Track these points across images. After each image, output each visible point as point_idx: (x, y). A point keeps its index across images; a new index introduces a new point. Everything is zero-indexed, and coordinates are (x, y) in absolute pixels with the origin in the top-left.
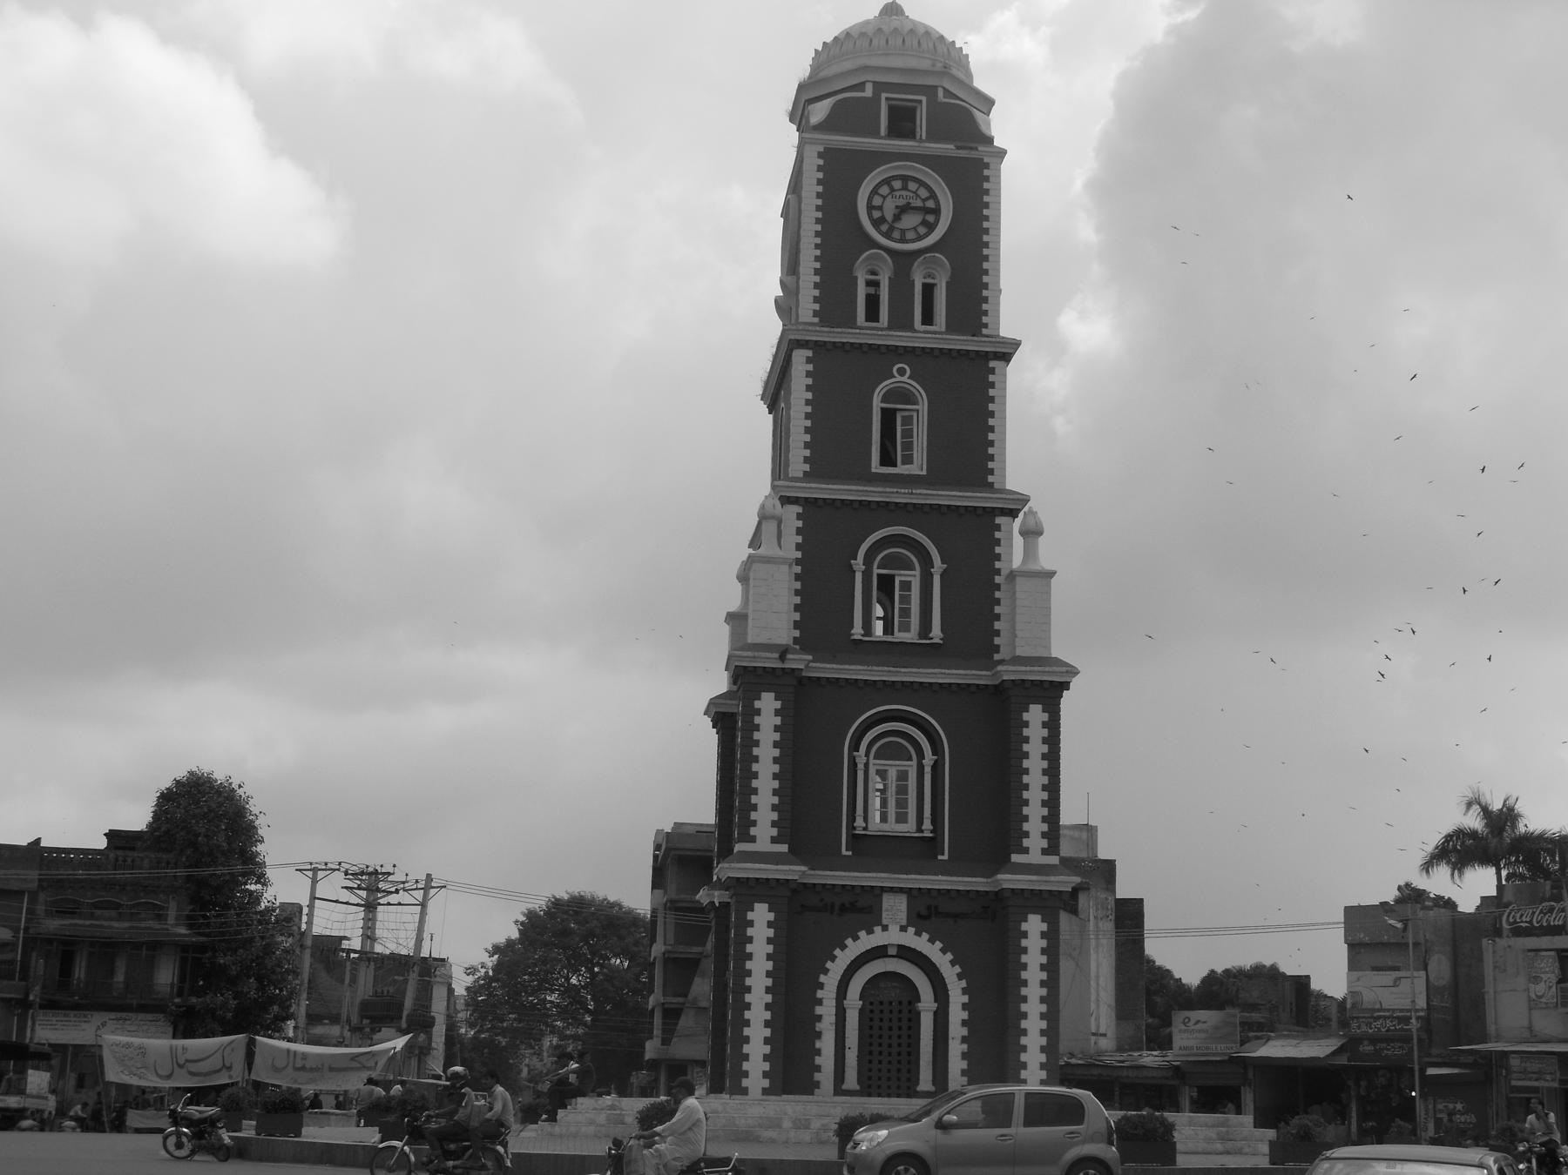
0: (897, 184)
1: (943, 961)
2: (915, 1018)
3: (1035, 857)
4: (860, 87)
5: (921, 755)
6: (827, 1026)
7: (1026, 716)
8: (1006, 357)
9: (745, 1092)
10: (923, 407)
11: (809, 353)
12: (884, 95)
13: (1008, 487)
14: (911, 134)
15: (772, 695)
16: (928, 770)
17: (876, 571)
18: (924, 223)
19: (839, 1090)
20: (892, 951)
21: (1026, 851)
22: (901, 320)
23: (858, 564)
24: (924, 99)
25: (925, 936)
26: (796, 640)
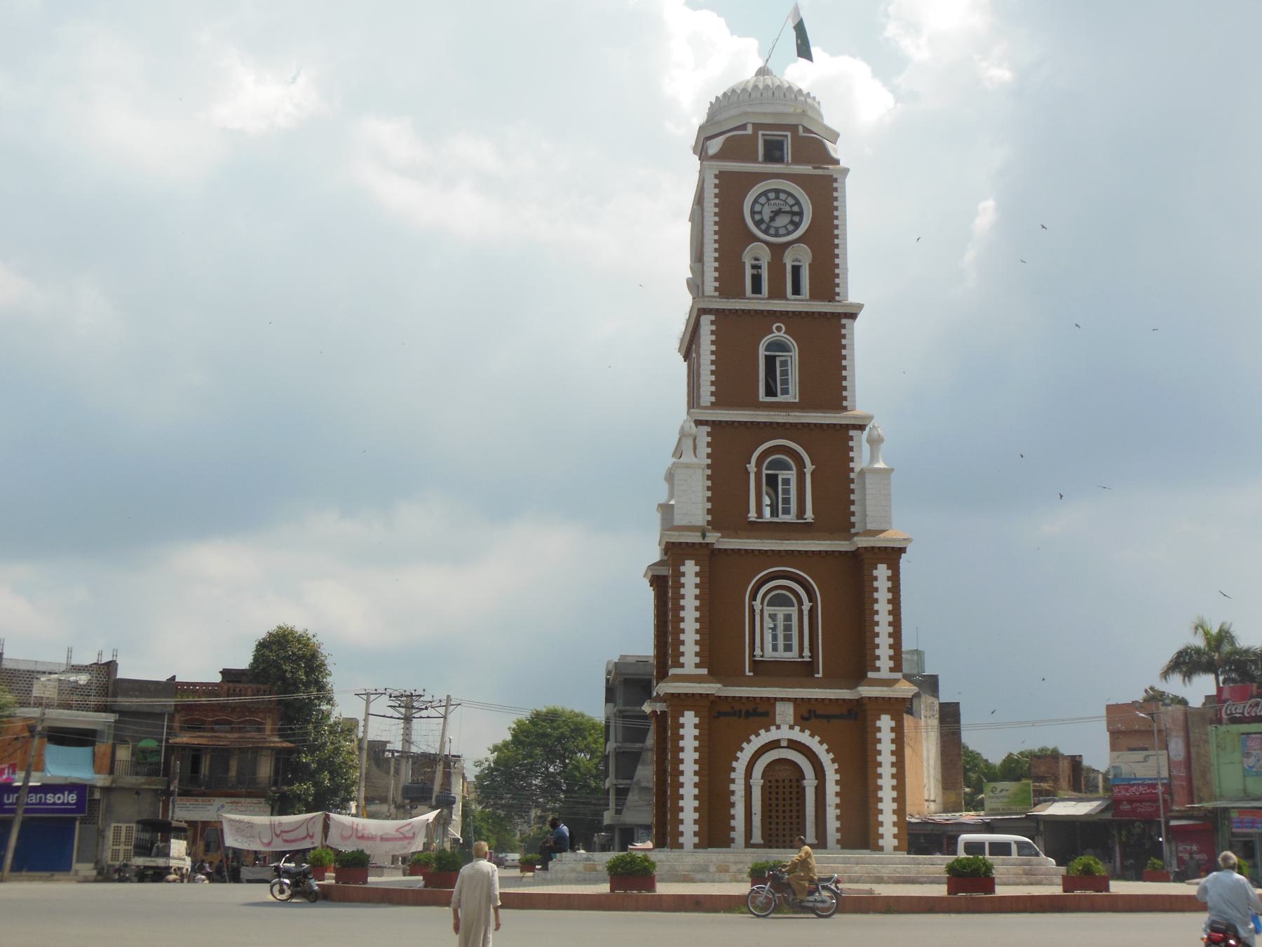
0: (772, 195)
1: (821, 750)
2: (802, 790)
3: (884, 674)
4: (743, 127)
7: (875, 573)
8: (853, 316)
9: (681, 846)
10: (795, 353)
11: (713, 317)
12: (760, 133)
14: (780, 160)
16: (806, 613)
17: (765, 472)
18: (792, 222)
19: (748, 844)
20: (784, 744)
21: (878, 669)
23: (752, 467)
24: (789, 134)
25: (807, 732)
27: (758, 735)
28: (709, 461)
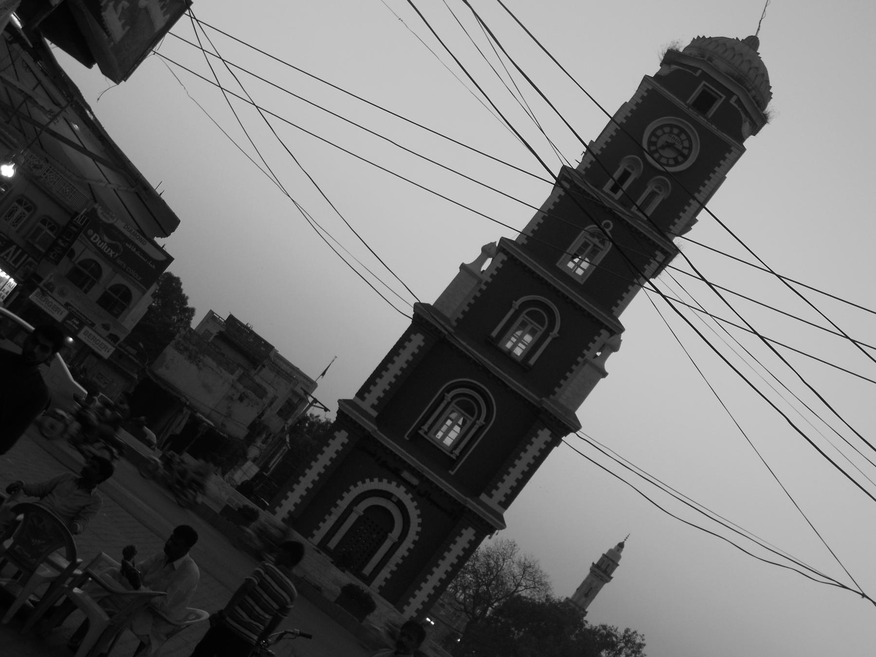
0: (676, 131)
2: (385, 537)
3: (493, 503)
4: (696, 69)
5: (478, 418)
6: (337, 513)
7: (540, 432)
9: (274, 513)
12: (704, 82)
13: (619, 319)
16: (477, 427)
18: (675, 159)
21: (491, 496)
22: (628, 201)
23: (517, 304)
24: (724, 97)
25: (415, 504)
26: (458, 320)
28: (490, 280)
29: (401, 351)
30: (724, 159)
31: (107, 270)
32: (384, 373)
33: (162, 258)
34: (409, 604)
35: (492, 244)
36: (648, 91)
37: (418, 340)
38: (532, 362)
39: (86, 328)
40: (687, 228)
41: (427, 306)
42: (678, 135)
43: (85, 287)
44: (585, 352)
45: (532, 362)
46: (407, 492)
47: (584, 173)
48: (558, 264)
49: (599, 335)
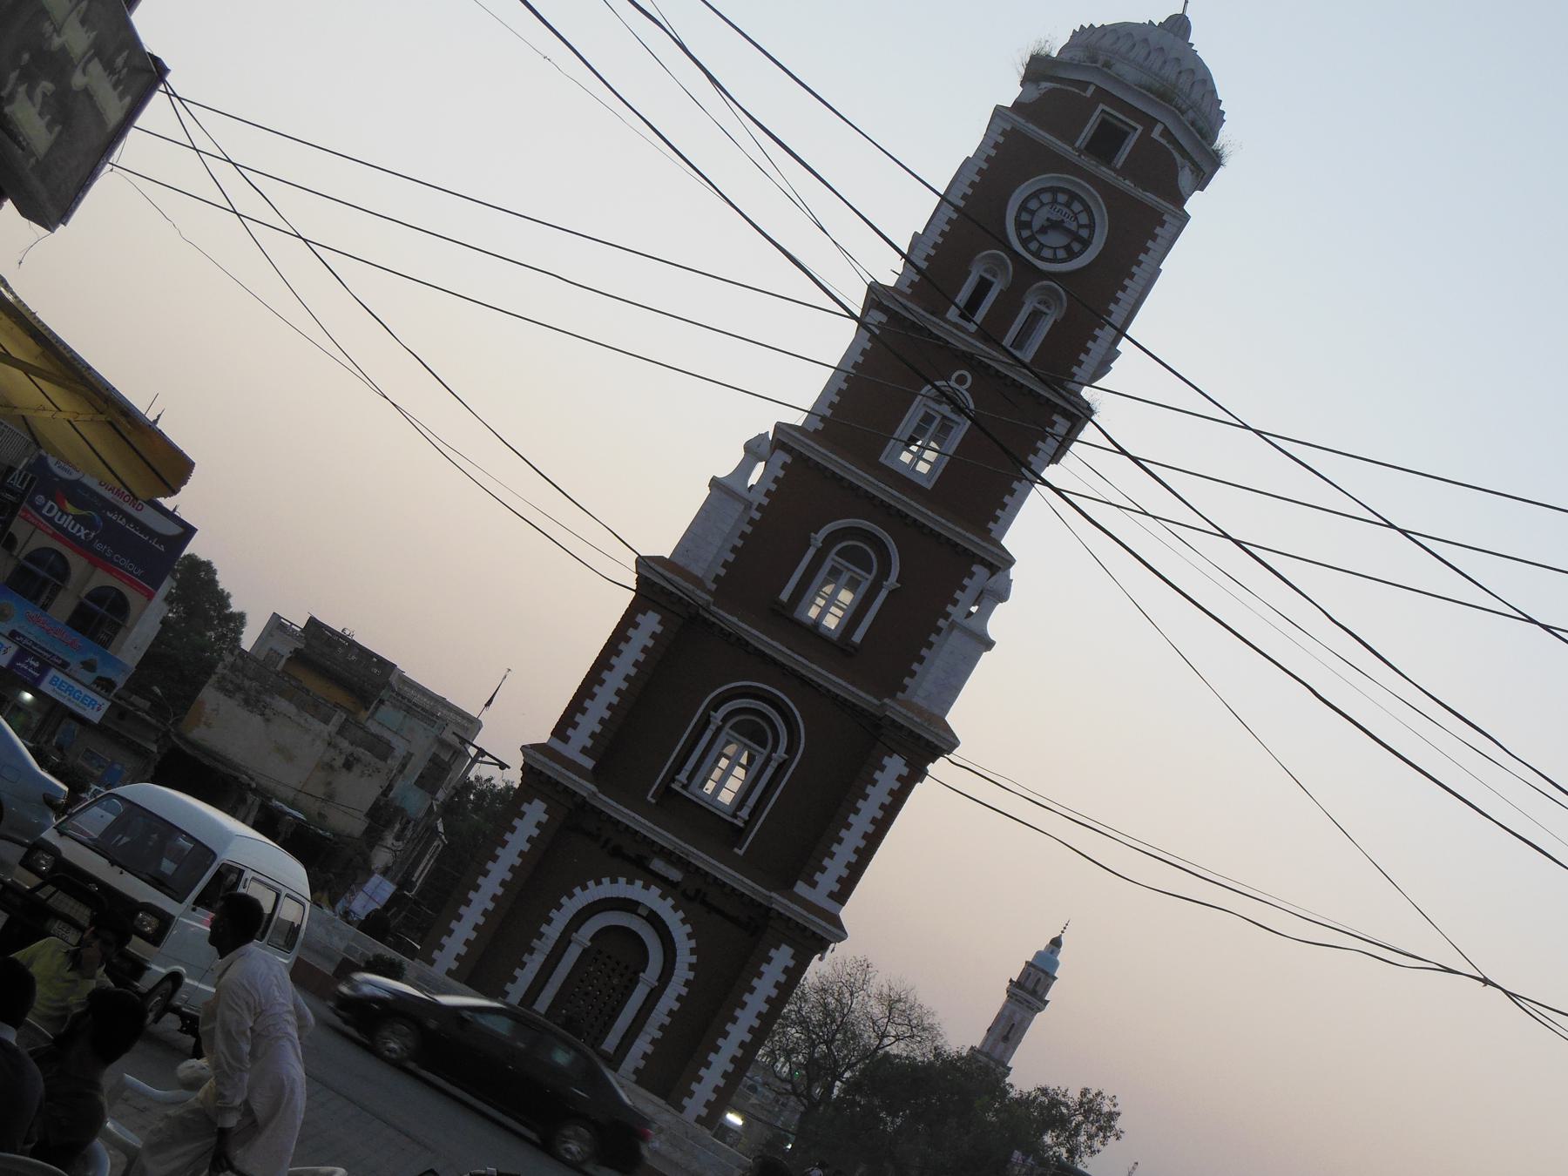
0: (1062, 198)
2: (634, 981)
3: (818, 896)
5: (775, 748)
6: (543, 947)
9: (431, 962)
12: (1101, 106)
13: (1006, 542)
15: (657, 617)
18: (1068, 248)
20: (640, 911)
21: (814, 885)
23: (818, 538)
24: (1140, 128)
25: (681, 914)
26: (717, 579)
27: (614, 881)
28: (765, 501)
29: (622, 646)
30: (1154, 238)
31: (77, 564)
32: (596, 689)
33: (176, 530)
34: (691, 1094)
35: (763, 436)
36: (1004, 133)
37: (651, 622)
38: (857, 637)
39: (53, 672)
40: (1103, 368)
41: (659, 560)
42: (1068, 205)
43: (43, 598)
44: (950, 608)
45: (857, 637)
46: (663, 897)
47: (909, 291)
48: (881, 459)
49: (971, 575)
